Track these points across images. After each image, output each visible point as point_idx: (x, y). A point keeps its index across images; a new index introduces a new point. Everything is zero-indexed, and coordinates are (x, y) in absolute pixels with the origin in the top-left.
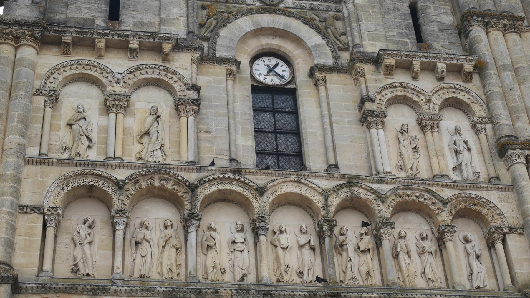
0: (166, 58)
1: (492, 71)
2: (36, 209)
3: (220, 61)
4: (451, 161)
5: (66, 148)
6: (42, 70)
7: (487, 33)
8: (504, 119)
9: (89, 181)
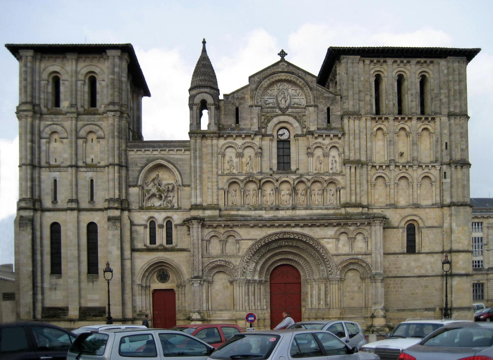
0: (252, 139)
1: (347, 136)
2: (222, 189)
3: (268, 135)
4: (330, 167)
5: (228, 170)
6: (220, 146)
7: (349, 121)
8: (347, 153)
9: (234, 180)
